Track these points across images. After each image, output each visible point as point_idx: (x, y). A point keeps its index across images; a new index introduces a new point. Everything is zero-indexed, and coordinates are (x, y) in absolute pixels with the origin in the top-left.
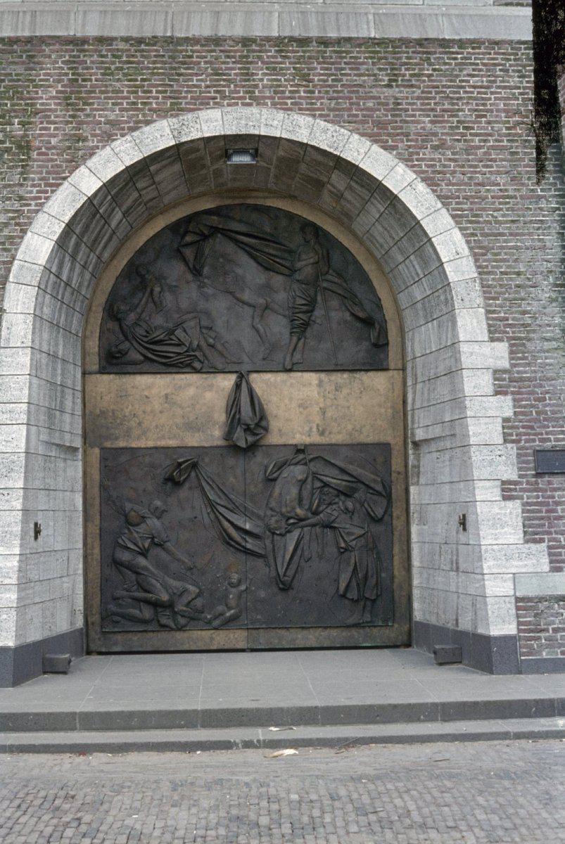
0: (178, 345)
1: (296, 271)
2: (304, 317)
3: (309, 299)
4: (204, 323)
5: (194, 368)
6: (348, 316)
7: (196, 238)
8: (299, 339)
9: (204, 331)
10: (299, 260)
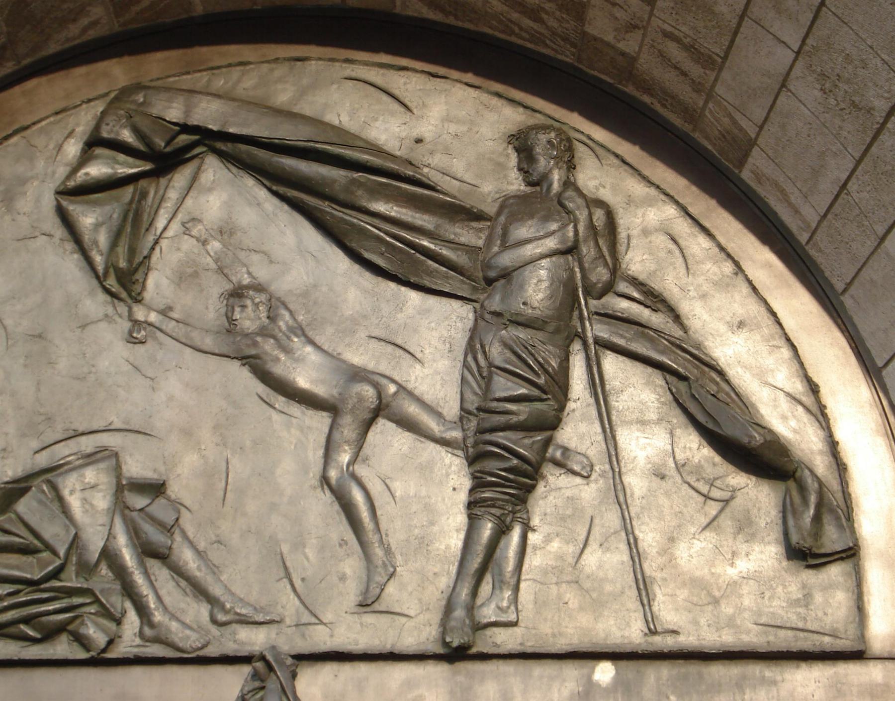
0: (25, 550)
1: (490, 282)
2: (525, 444)
3: (541, 381)
4: (136, 467)
5: (81, 640)
6: (693, 447)
7: (127, 167)
8: (502, 531)
9: (139, 501)
10: (505, 246)
